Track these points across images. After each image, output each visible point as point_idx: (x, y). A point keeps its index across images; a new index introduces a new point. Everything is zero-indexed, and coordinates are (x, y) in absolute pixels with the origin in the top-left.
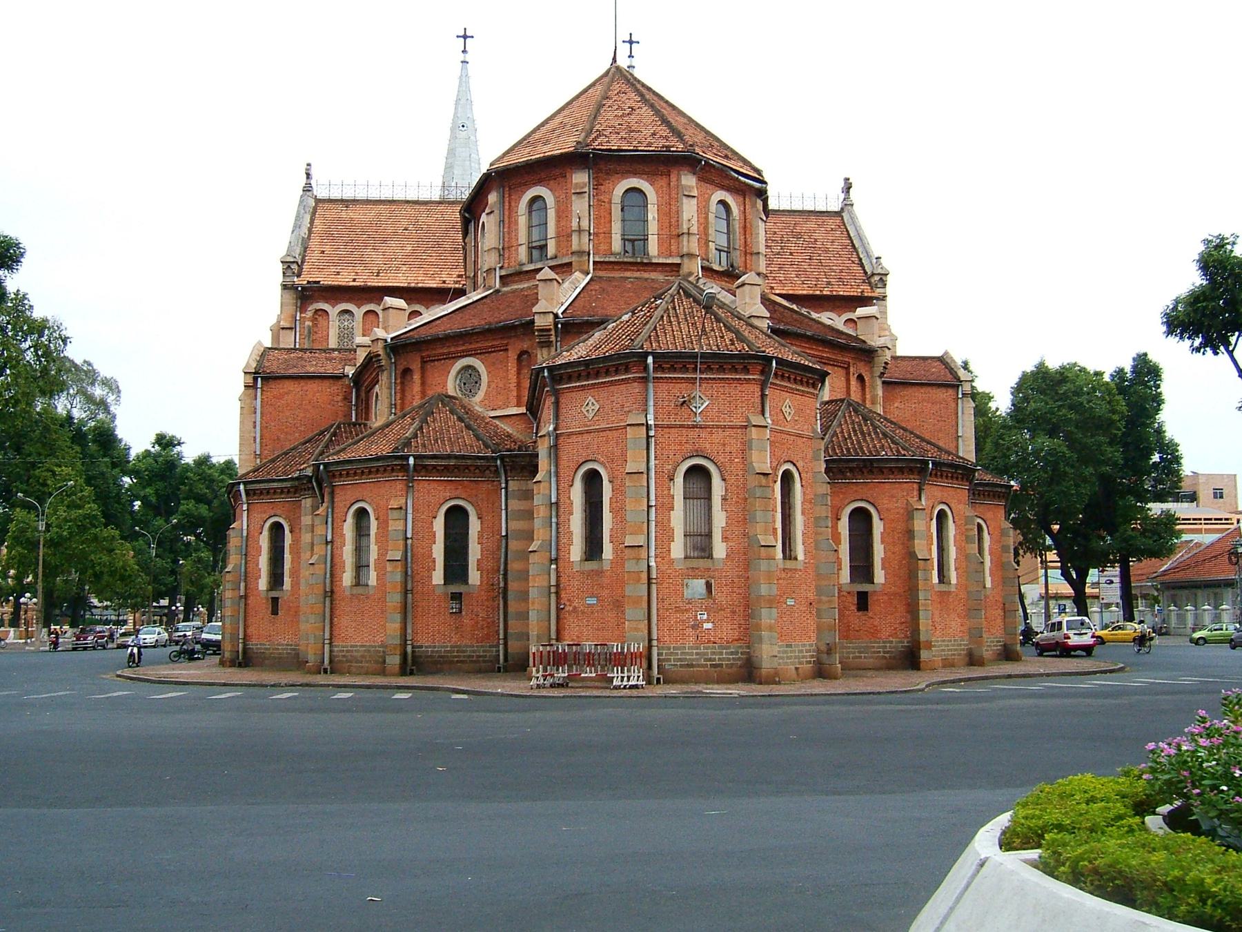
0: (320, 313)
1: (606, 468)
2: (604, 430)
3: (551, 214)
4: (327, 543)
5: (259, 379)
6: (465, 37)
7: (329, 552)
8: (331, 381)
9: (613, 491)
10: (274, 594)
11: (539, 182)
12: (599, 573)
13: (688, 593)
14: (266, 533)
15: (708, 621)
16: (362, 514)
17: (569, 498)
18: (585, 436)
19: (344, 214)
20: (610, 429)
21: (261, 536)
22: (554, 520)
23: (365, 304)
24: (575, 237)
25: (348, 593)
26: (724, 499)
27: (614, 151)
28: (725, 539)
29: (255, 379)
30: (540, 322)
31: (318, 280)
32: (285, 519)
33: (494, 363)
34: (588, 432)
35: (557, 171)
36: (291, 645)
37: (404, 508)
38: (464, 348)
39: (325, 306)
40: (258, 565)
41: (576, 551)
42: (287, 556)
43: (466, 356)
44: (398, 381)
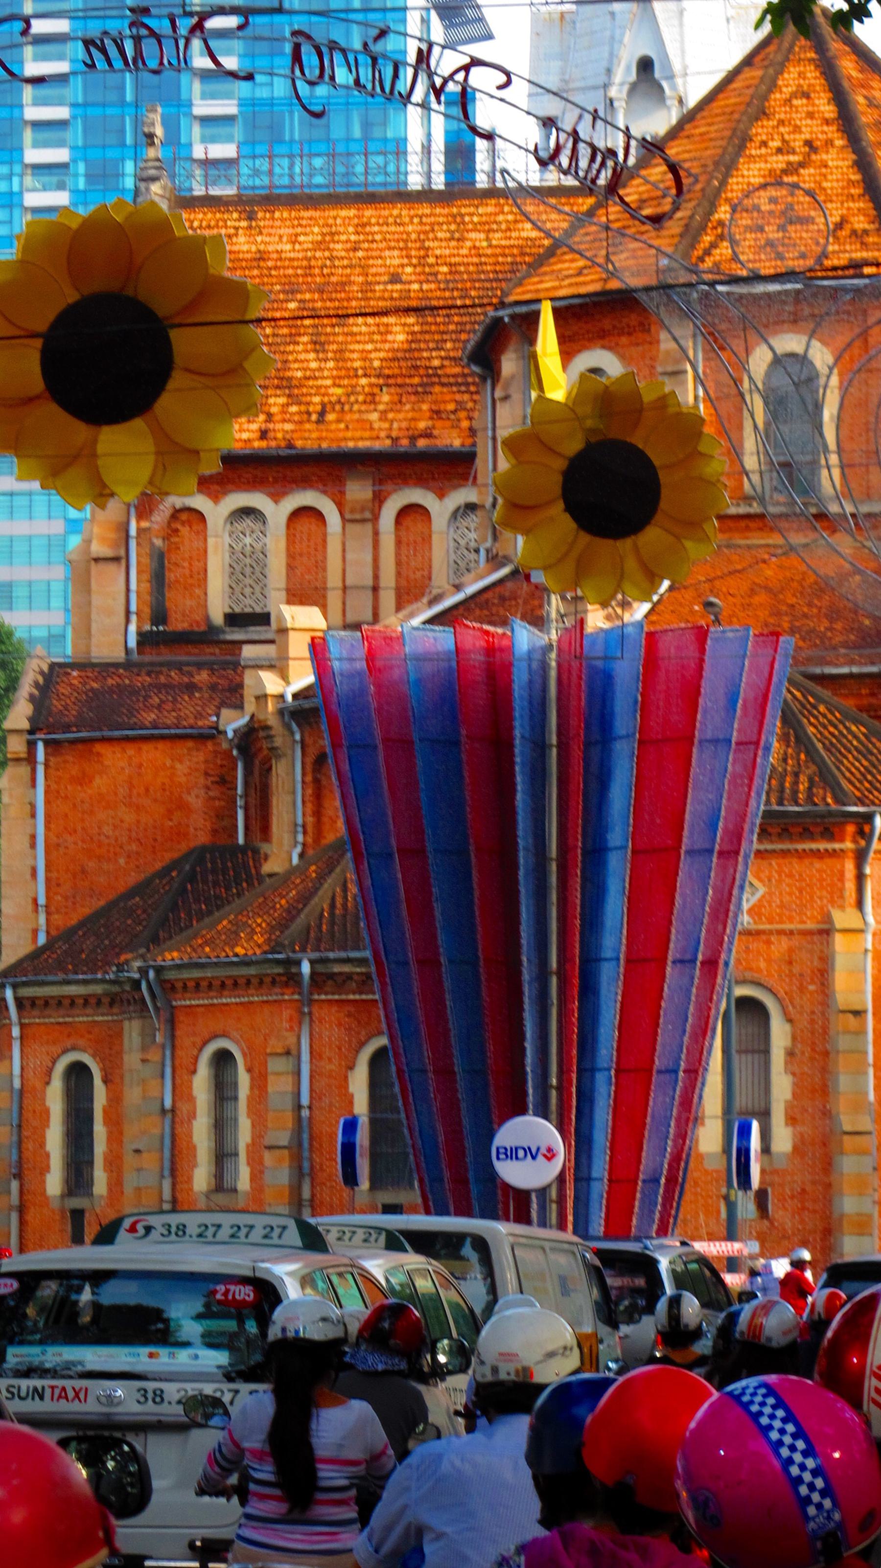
0: (184, 516)
7: (167, 1130)
16: (223, 1059)
26: (790, 1054)
28: (791, 1120)
29: (31, 745)
37: (294, 1052)
39: (200, 502)
40: (42, 1145)
44: (309, 778)
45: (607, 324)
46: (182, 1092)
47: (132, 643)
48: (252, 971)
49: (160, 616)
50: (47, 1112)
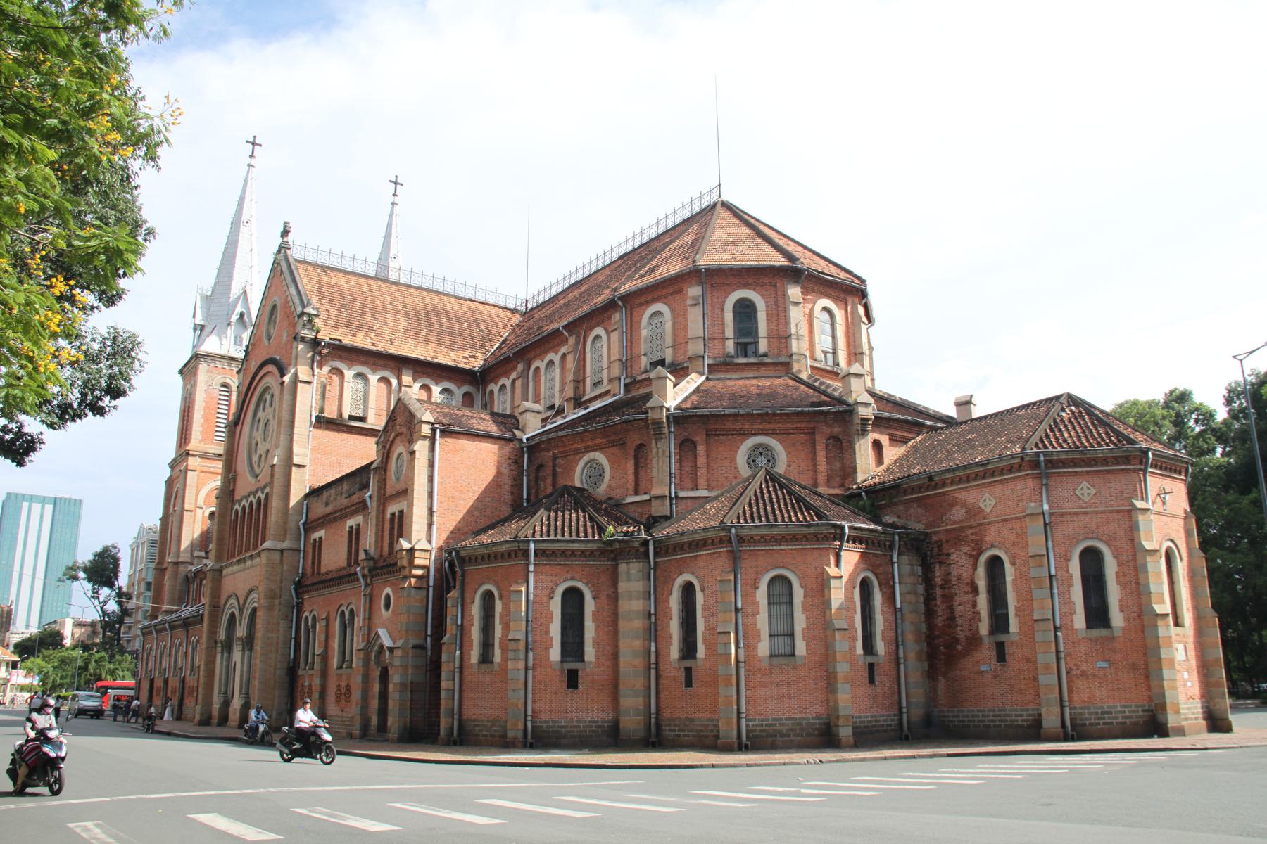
1: (1109, 545)
2: (1103, 512)
4: (737, 610)
5: (438, 430)
6: (254, 144)
8: (503, 442)
9: (1119, 566)
10: (573, 666)
11: (746, 285)
12: (1112, 638)
14: (558, 598)
15: (1189, 680)
17: (1067, 571)
18: (1082, 517)
19: (325, 278)
20: (1111, 512)
21: (552, 602)
22: (1055, 591)
23: (379, 370)
25: (765, 664)
27: (820, 272)
29: (434, 430)
30: (863, 412)
31: (339, 338)
32: (586, 584)
33: (794, 444)
34: (1086, 513)
35: (766, 280)
36: (598, 722)
38: (760, 426)
40: (547, 632)
41: (1079, 621)
43: (759, 434)
45: (750, 280)
46: (750, 599)
47: (313, 419)
48: (812, 530)
49: (322, 410)
50: (551, 614)
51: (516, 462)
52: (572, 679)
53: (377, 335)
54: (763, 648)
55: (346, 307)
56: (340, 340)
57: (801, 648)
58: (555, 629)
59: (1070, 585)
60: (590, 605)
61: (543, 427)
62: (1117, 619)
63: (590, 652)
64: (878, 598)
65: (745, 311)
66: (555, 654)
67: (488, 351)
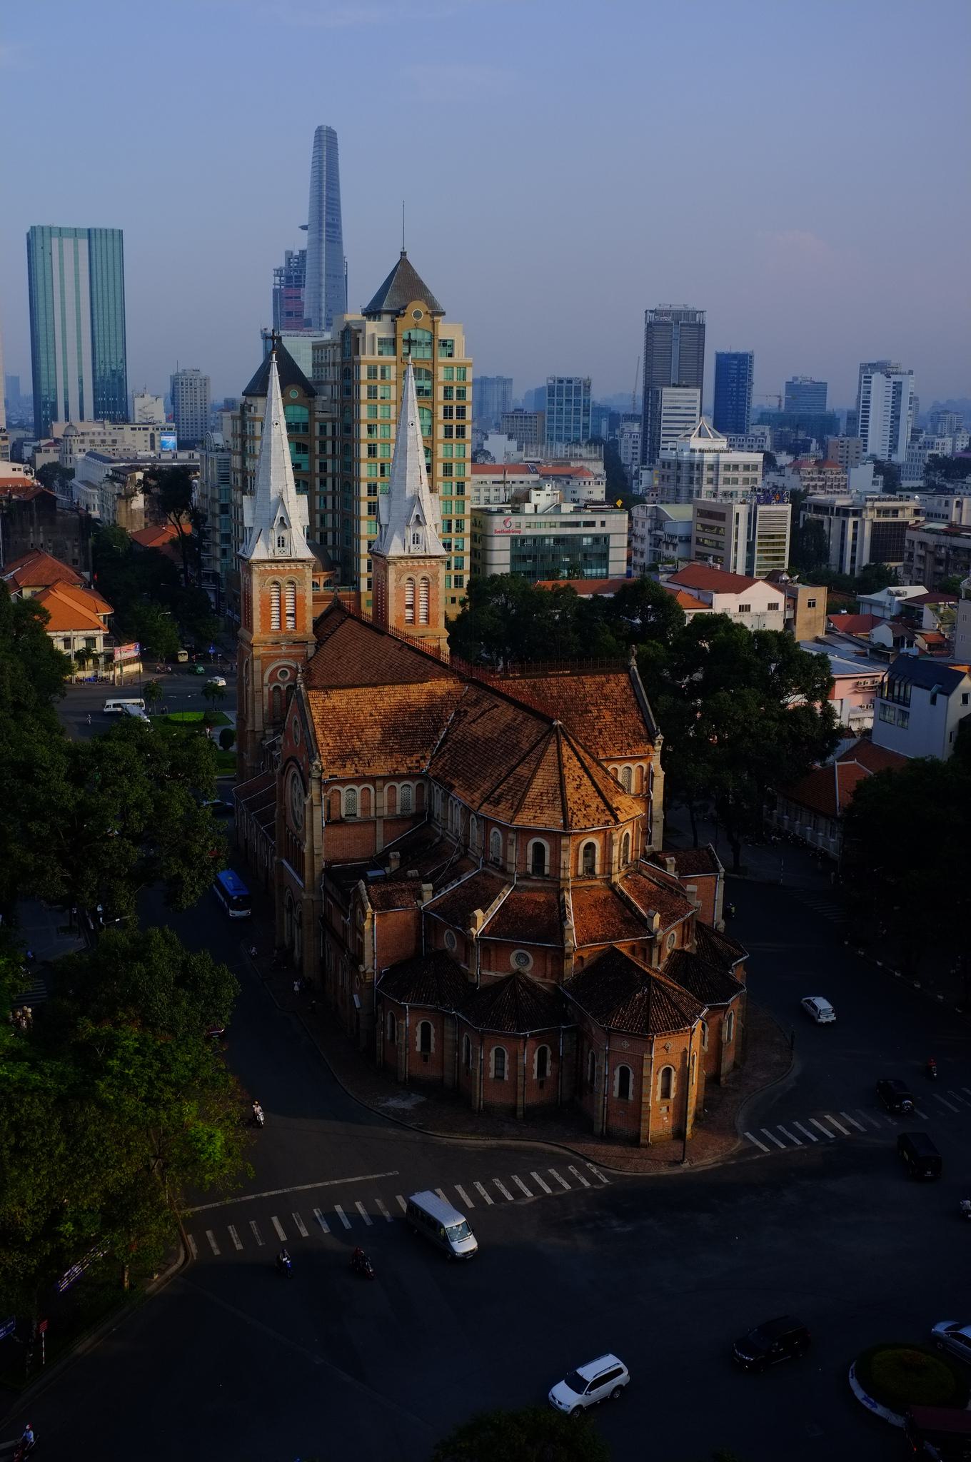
3: (547, 854)
4: (481, 1060)
13: (662, 1112)
24: (562, 871)
39: (339, 788)
41: (616, 1094)
42: (432, 1038)
46: (487, 1054)
49: (329, 817)
51: (418, 918)
52: (426, 1059)
53: (360, 759)
54: (492, 1075)
55: (340, 734)
56: (336, 776)
57: (506, 1077)
58: (418, 1038)
59: (614, 1079)
60: (433, 1031)
61: (434, 896)
62: (631, 1097)
63: (433, 1049)
64: (549, 1053)
65: (539, 849)
66: (418, 1048)
67: (435, 746)
